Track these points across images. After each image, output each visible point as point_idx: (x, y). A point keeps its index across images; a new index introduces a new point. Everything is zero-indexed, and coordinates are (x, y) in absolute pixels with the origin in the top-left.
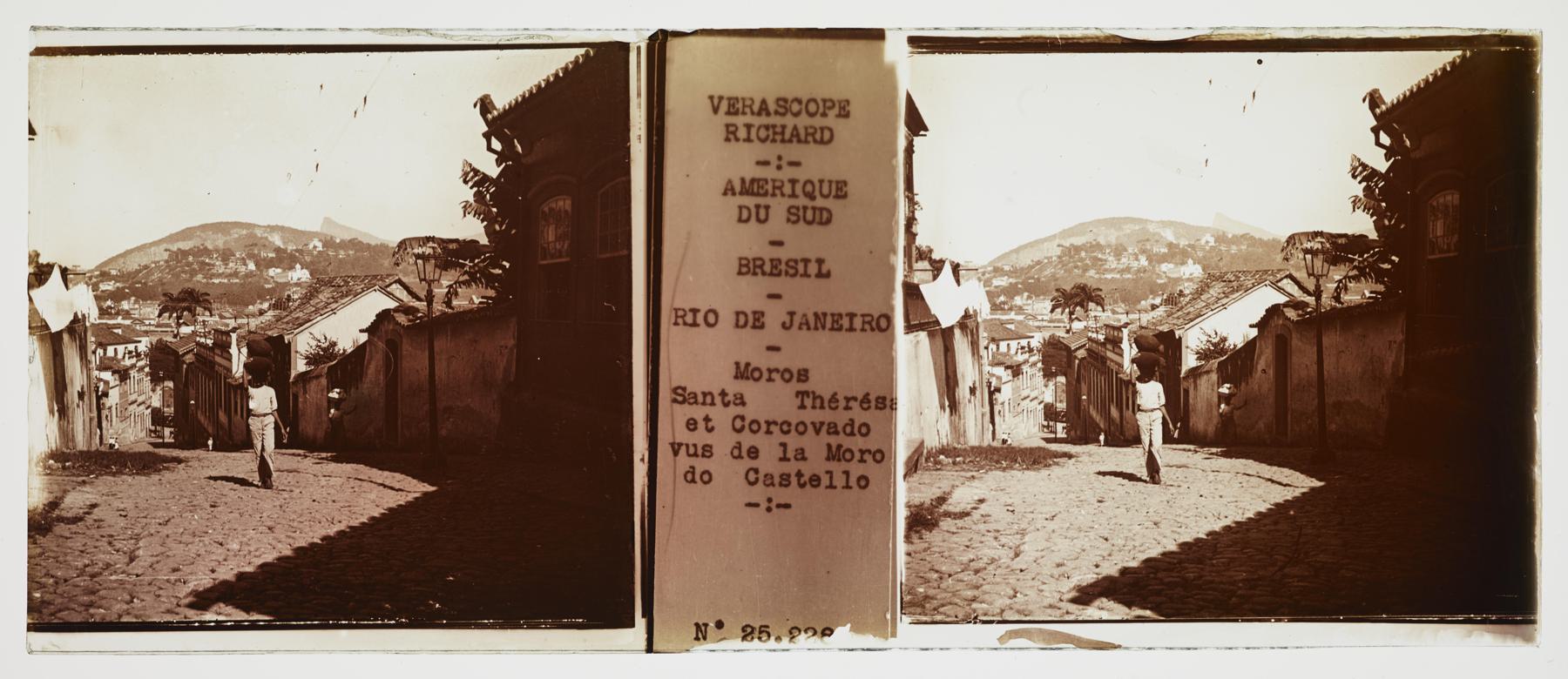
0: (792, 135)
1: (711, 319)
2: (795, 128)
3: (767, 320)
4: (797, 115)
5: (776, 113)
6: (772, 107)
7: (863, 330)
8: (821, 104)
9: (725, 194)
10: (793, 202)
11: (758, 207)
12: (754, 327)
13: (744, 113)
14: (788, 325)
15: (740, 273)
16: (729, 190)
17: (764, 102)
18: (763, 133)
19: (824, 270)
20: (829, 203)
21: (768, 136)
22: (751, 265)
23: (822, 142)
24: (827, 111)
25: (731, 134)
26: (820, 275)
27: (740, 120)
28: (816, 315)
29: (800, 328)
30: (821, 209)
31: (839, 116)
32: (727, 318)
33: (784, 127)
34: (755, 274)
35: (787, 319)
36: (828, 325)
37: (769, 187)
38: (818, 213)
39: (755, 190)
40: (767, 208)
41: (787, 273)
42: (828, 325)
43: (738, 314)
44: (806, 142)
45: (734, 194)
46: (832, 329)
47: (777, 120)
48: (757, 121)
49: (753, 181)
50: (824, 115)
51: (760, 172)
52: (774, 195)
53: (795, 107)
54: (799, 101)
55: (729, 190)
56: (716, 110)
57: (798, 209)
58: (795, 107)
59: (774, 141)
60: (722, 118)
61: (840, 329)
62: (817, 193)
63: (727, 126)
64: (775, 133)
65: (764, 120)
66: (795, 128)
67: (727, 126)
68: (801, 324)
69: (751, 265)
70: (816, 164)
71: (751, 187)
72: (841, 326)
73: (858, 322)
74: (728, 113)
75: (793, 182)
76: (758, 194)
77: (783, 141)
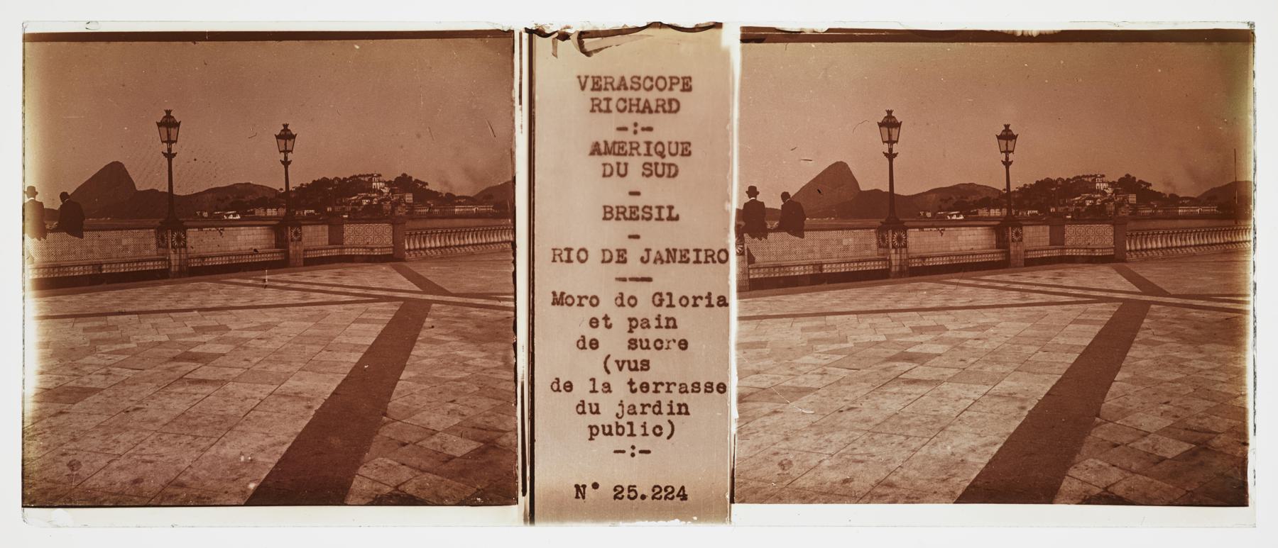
0: (645, 107)
1: (583, 256)
2: (647, 101)
5: (632, 88)
6: (629, 84)
8: (668, 81)
9: (592, 154)
12: (618, 262)
13: (606, 89)
14: (645, 259)
15: (605, 218)
16: (596, 150)
17: (623, 79)
18: (622, 105)
19: (674, 215)
20: (677, 160)
21: (625, 107)
22: (615, 212)
23: (670, 111)
25: (595, 107)
26: (670, 218)
27: (602, 95)
28: (668, 250)
29: (655, 262)
30: (670, 165)
31: (683, 90)
32: (595, 256)
33: (639, 100)
34: (618, 219)
35: (645, 255)
36: (678, 258)
37: (627, 148)
38: (666, 167)
39: (616, 151)
40: (626, 164)
42: (678, 258)
43: (604, 251)
44: (657, 111)
45: (600, 154)
46: (680, 262)
48: (615, 95)
49: (614, 143)
52: (631, 154)
54: (651, 79)
55: (596, 150)
56: (583, 88)
57: (651, 165)
58: (648, 84)
59: (630, 111)
60: (589, 93)
61: (687, 261)
62: (666, 152)
63: (593, 99)
64: (631, 105)
65: (623, 94)
66: (647, 101)
67: (593, 99)
69: (615, 212)
70: (666, 129)
73: (702, 256)
74: (593, 89)
75: (648, 143)
76: (619, 154)
77: (638, 111)
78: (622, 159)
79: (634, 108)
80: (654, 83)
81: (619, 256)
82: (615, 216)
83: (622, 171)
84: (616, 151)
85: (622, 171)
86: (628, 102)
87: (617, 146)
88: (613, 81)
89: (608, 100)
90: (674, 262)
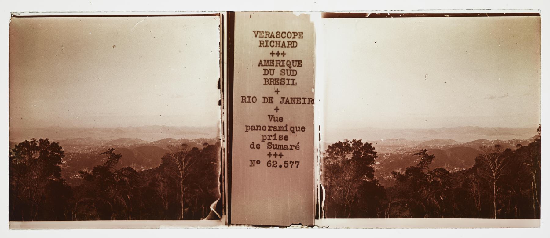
2: (284, 42)
6: (275, 35)
9: (259, 66)
11: (270, 70)
12: (269, 103)
13: (266, 37)
14: (282, 102)
15: (265, 84)
17: (272, 33)
19: (295, 83)
21: (274, 45)
22: (269, 81)
23: (293, 47)
24: (295, 37)
26: (293, 84)
28: (291, 98)
29: (286, 103)
30: (293, 70)
31: (299, 38)
33: (280, 41)
34: (271, 84)
36: (296, 102)
37: (275, 63)
40: (274, 70)
41: (281, 84)
42: (296, 102)
44: (288, 47)
45: (262, 65)
46: (297, 103)
48: (270, 40)
49: (268, 61)
50: (294, 38)
52: (277, 66)
53: (284, 35)
54: (285, 33)
55: (260, 64)
56: (256, 36)
57: (284, 70)
59: (276, 47)
60: (258, 39)
63: (260, 41)
65: (272, 39)
66: (284, 42)
67: (260, 41)
68: (286, 102)
69: (269, 81)
70: (291, 54)
71: (267, 62)
72: (301, 102)
74: (260, 37)
75: (283, 61)
76: (270, 65)
77: (279, 46)
78: (272, 68)
79: (278, 45)
80: (286, 35)
82: (270, 83)
83: (272, 73)
85: (272, 73)
86: (275, 42)
87: (269, 62)
89: (267, 41)
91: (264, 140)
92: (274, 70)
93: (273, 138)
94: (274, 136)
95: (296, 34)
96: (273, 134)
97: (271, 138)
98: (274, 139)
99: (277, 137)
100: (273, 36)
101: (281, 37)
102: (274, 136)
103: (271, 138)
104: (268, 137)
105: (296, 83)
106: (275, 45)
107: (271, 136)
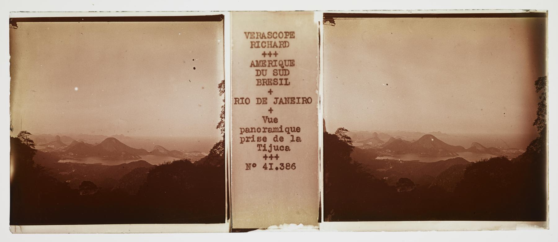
1: (248, 101)
2: (275, 43)
3: (268, 101)
4: (276, 38)
5: (268, 38)
6: (266, 36)
7: (303, 103)
8: (284, 34)
9: (251, 66)
10: (275, 68)
11: (263, 70)
13: (257, 38)
14: (276, 102)
15: (258, 85)
16: (252, 65)
17: (263, 33)
18: (264, 45)
19: (288, 83)
20: (288, 68)
21: (265, 46)
23: (285, 47)
24: (287, 37)
26: (286, 84)
28: (285, 98)
29: (280, 103)
30: (285, 70)
31: (291, 37)
32: (253, 101)
33: (271, 42)
34: (263, 85)
35: (275, 100)
36: (290, 101)
37: (267, 63)
38: (284, 71)
40: (266, 70)
41: (274, 84)
42: (290, 101)
43: (258, 99)
44: (280, 47)
45: (254, 66)
46: (291, 103)
47: (270, 40)
48: (261, 40)
50: (286, 38)
51: (262, 58)
52: (269, 66)
53: (275, 35)
54: (276, 33)
55: (252, 65)
56: (247, 38)
57: (277, 70)
59: (268, 47)
60: (250, 40)
61: (295, 103)
63: (252, 42)
64: (268, 44)
65: (264, 40)
66: (275, 43)
67: (252, 42)
69: (262, 82)
70: (284, 54)
73: (301, 100)
74: (251, 38)
75: (275, 61)
76: (263, 66)
77: (271, 47)
79: (270, 46)
80: (278, 35)
81: (263, 101)
82: (262, 84)
84: (261, 65)
85: (264, 74)
88: (261, 34)
89: (258, 42)
90: (289, 103)
91: (242, 142)
92: (266, 70)
93: (252, 139)
94: (252, 137)
95: (287, 34)
96: (251, 136)
97: (249, 139)
98: (252, 141)
99: (256, 139)
100: (265, 36)
101: (273, 38)
102: (252, 137)
103: (249, 139)
104: (246, 139)
105: (289, 83)
106: (267, 46)
107: (250, 138)
